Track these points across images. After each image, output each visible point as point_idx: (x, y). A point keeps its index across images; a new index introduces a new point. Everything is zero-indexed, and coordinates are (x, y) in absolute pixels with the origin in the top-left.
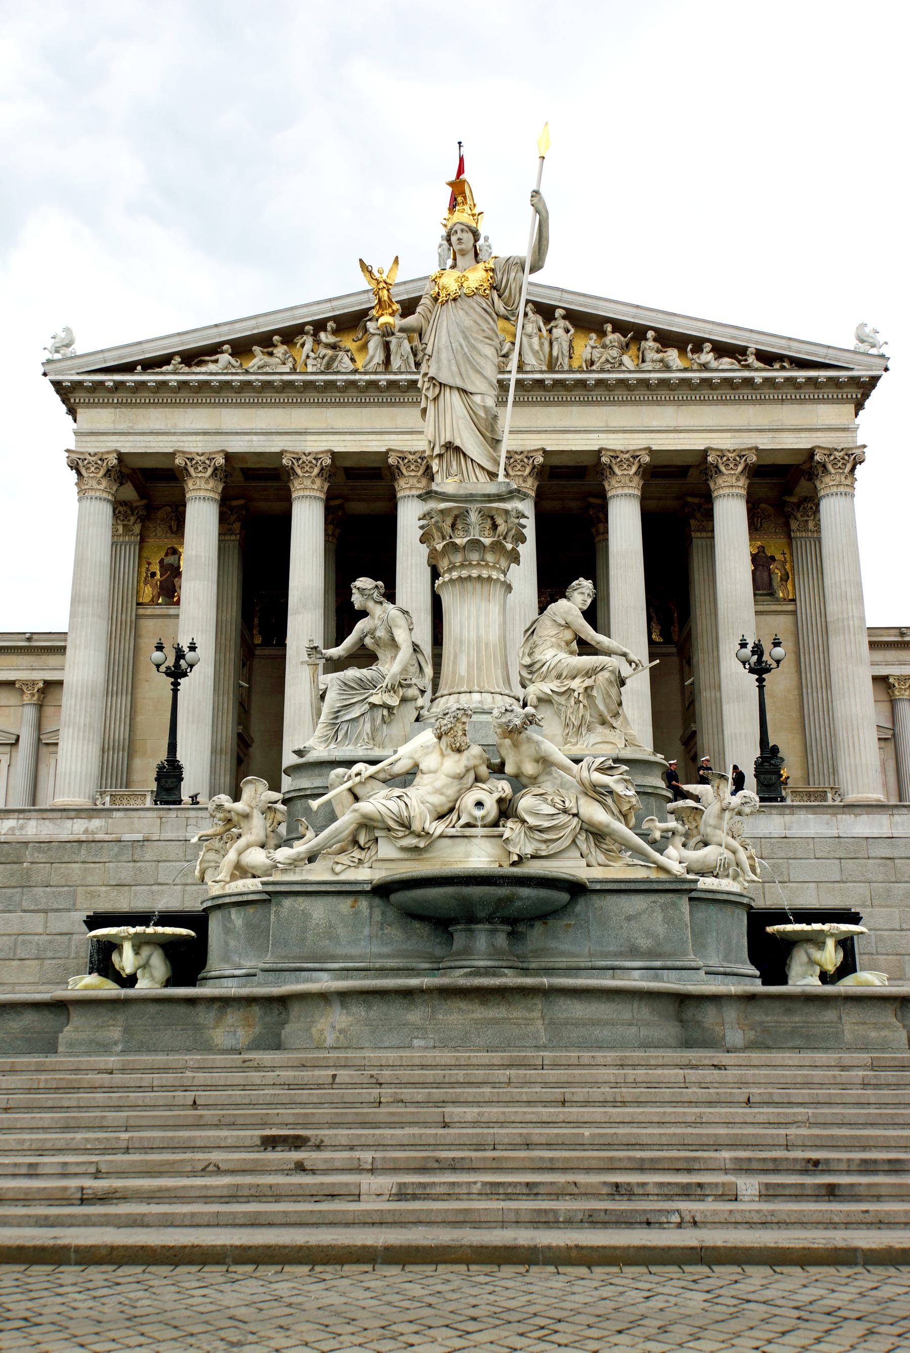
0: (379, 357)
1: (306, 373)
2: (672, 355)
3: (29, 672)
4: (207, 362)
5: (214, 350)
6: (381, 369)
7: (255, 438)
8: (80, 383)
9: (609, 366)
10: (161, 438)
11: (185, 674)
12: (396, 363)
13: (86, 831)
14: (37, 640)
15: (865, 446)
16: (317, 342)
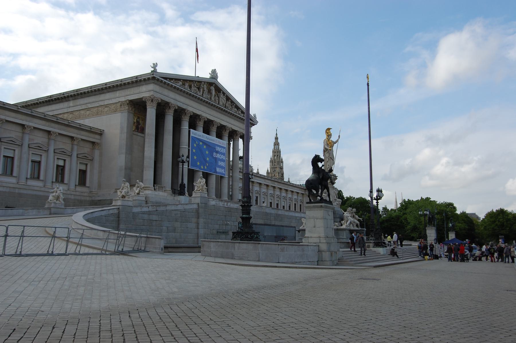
0: (202, 94)
1: (192, 92)
2: (236, 110)
3: (77, 135)
4: (176, 82)
5: (179, 80)
6: (202, 96)
7: (181, 103)
8: (159, 79)
9: (230, 109)
10: (167, 97)
11: (185, 162)
12: (204, 96)
13: (237, 207)
14: (82, 127)
15: (252, 137)
16: (194, 85)
